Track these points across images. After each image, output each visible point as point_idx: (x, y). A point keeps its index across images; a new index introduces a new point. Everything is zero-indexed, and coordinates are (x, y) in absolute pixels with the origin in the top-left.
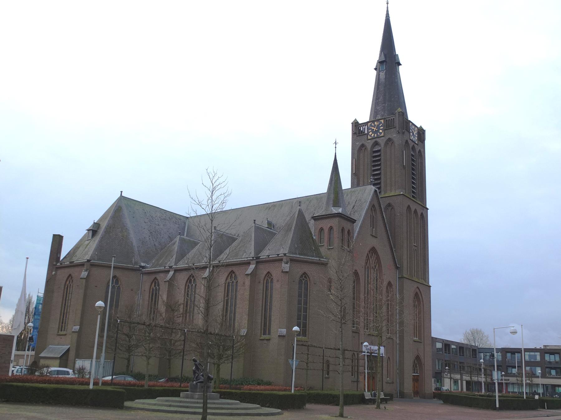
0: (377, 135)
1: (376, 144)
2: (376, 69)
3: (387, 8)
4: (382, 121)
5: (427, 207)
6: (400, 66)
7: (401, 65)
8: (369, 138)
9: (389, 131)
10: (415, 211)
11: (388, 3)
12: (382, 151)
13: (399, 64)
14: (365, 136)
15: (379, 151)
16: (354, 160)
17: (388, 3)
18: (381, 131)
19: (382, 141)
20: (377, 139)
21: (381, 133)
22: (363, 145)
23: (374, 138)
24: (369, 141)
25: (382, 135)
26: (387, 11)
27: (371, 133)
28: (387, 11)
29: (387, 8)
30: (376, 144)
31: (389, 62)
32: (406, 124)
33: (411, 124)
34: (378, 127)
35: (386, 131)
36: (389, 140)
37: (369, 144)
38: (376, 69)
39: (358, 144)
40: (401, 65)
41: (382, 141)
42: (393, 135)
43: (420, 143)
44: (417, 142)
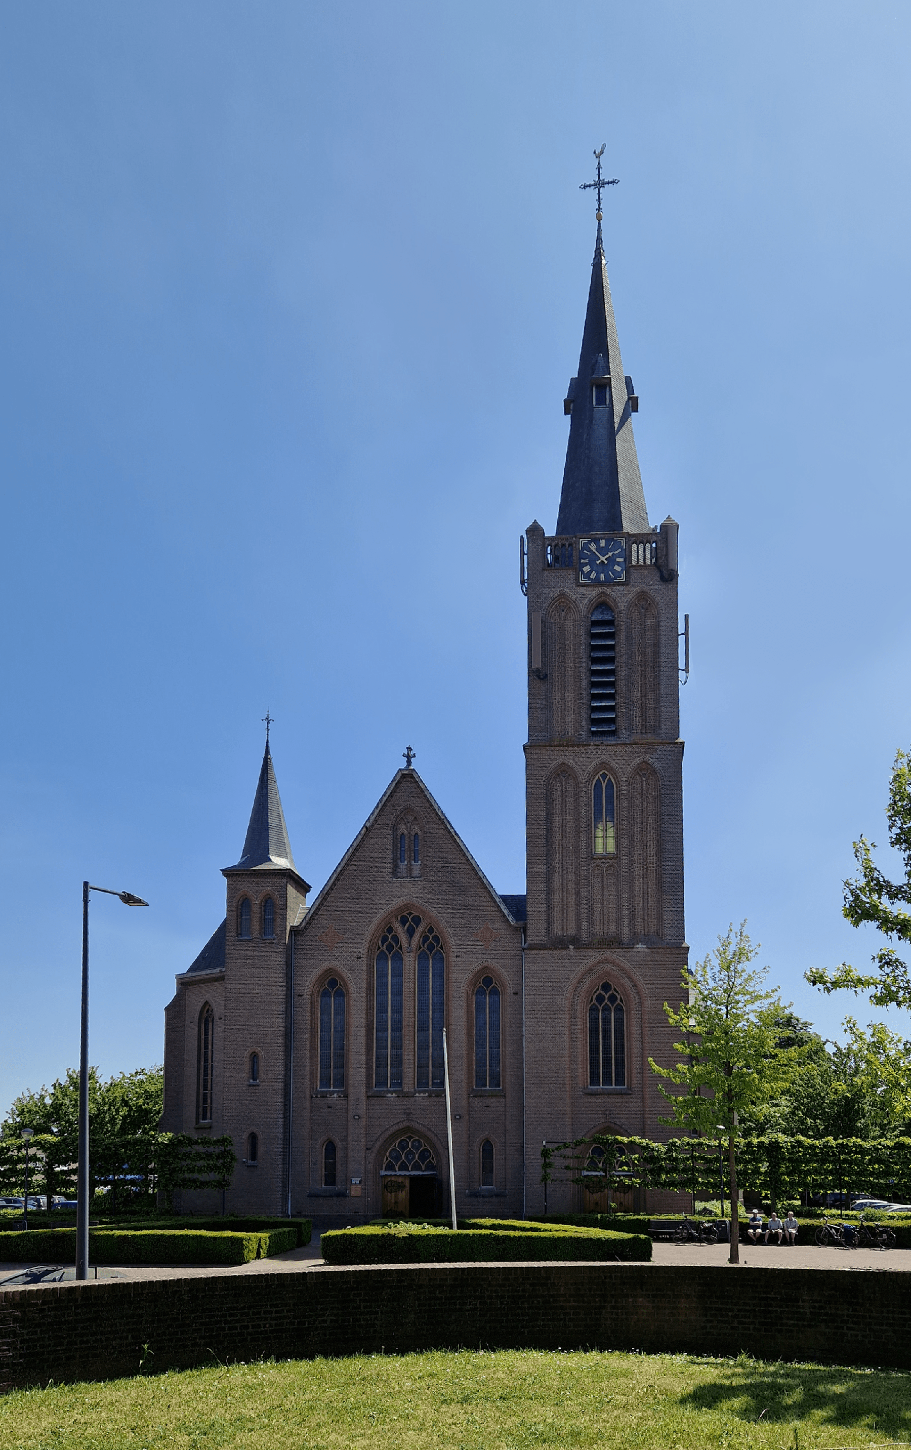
23: (597, 583)
24: (582, 590)
27: (586, 569)
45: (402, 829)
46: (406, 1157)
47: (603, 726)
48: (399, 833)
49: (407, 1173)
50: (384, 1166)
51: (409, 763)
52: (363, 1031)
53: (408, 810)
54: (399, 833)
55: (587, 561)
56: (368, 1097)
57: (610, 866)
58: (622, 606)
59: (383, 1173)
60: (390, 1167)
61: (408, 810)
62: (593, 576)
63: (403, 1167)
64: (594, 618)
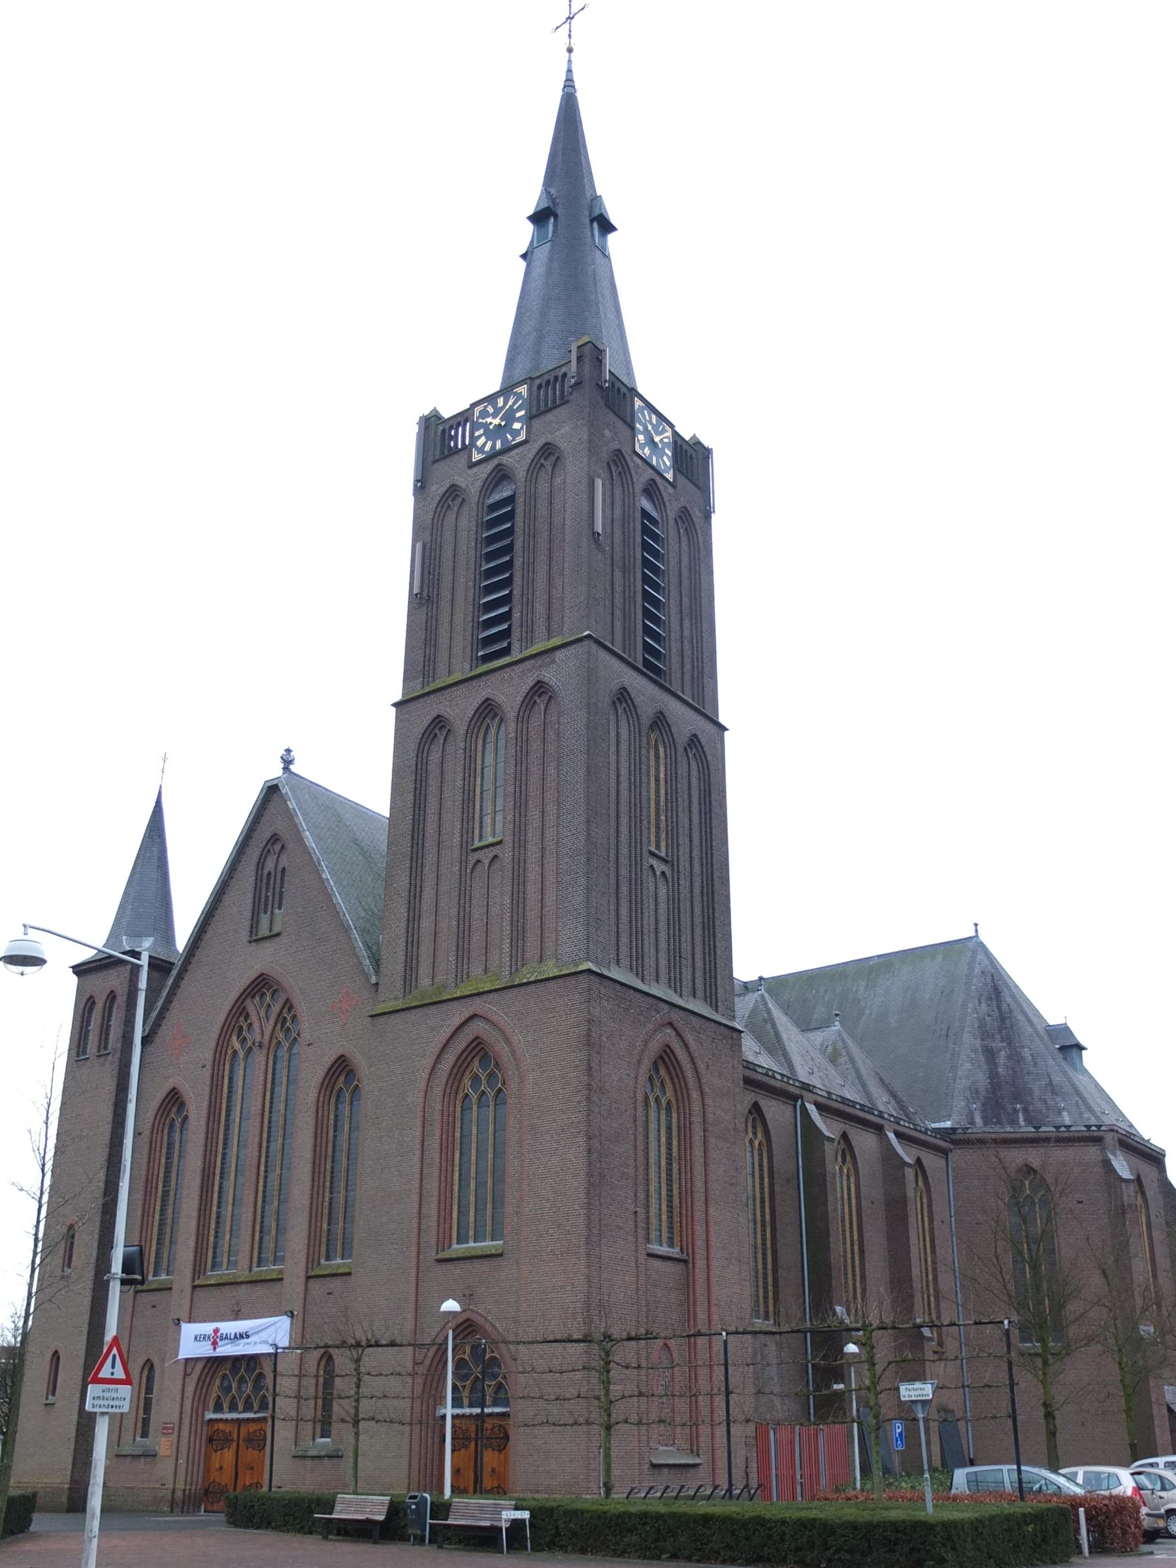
0: (504, 441)
1: (501, 476)
2: (524, 256)
3: (570, 61)
4: (523, 390)
5: (723, 719)
6: (611, 237)
7: (612, 229)
8: (476, 457)
9: (549, 416)
10: (660, 722)
11: (570, 50)
12: (520, 501)
13: (607, 227)
14: (464, 455)
15: (511, 500)
16: (419, 546)
17: (570, 50)
18: (517, 426)
19: (518, 463)
20: (505, 459)
21: (516, 433)
22: (454, 491)
24: (475, 470)
25: (522, 437)
26: (569, 71)
27: (479, 443)
28: (569, 71)
29: (570, 61)
30: (501, 476)
31: (570, 218)
32: (618, 399)
33: (638, 403)
34: (509, 417)
35: (534, 422)
36: (548, 450)
37: (472, 482)
38: (524, 256)
39: (437, 489)
40: (612, 229)
41: (518, 463)
42: (566, 430)
43: (682, 481)
44: (669, 476)
45: (270, 865)
46: (239, 1387)
47: (494, 643)
48: (266, 872)
49: (235, 1416)
50: (212, 1404)
51: (286, 769)
52: (198, 1180)
53: (275, 838)
54: (266, 872)
55: (482, 431)
56: (194, 1287)
57: (496, 857)
58: (521, 472)
59: (210, 1415)
60: (218, 1408)
61: (275, 838)
62: (487, 448)
63: (233, 1408)
64: (491, 501)
